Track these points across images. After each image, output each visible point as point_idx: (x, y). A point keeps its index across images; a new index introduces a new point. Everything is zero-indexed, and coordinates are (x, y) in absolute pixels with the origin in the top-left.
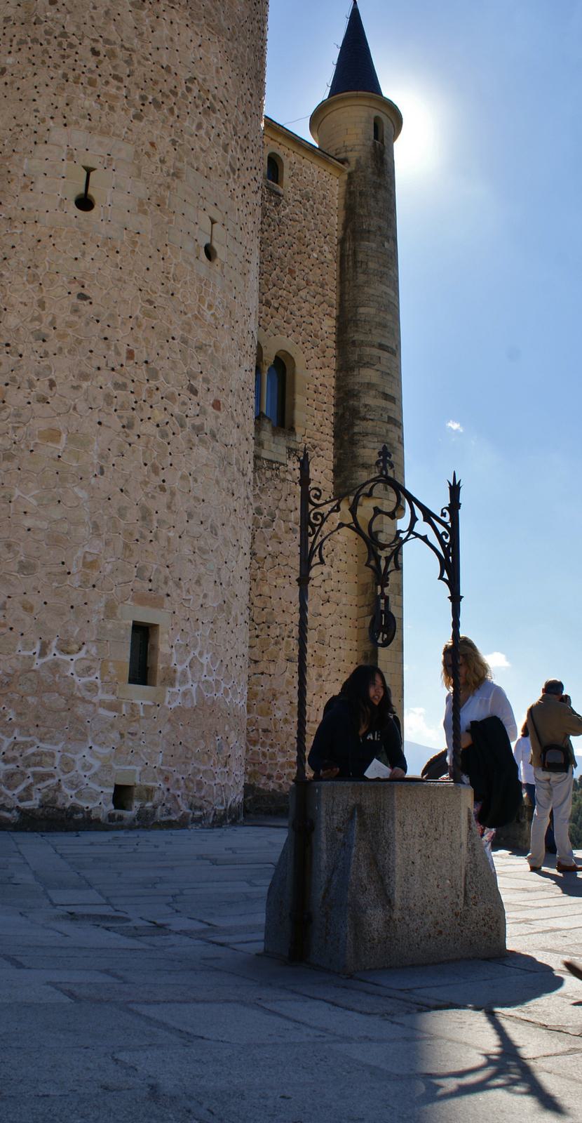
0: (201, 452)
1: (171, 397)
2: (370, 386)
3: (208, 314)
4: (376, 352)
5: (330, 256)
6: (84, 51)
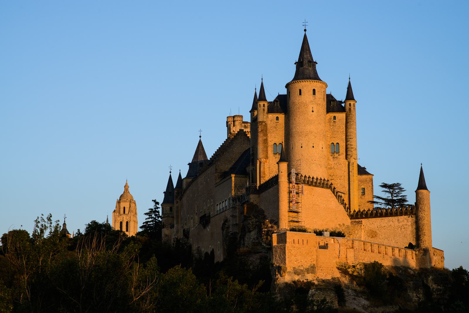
0: (313, 165)
1: (310, 161)
2: (349, 144)
3: (313, 153)
4: (349, 139)
5: (344, 127)
6: (300, 133)
